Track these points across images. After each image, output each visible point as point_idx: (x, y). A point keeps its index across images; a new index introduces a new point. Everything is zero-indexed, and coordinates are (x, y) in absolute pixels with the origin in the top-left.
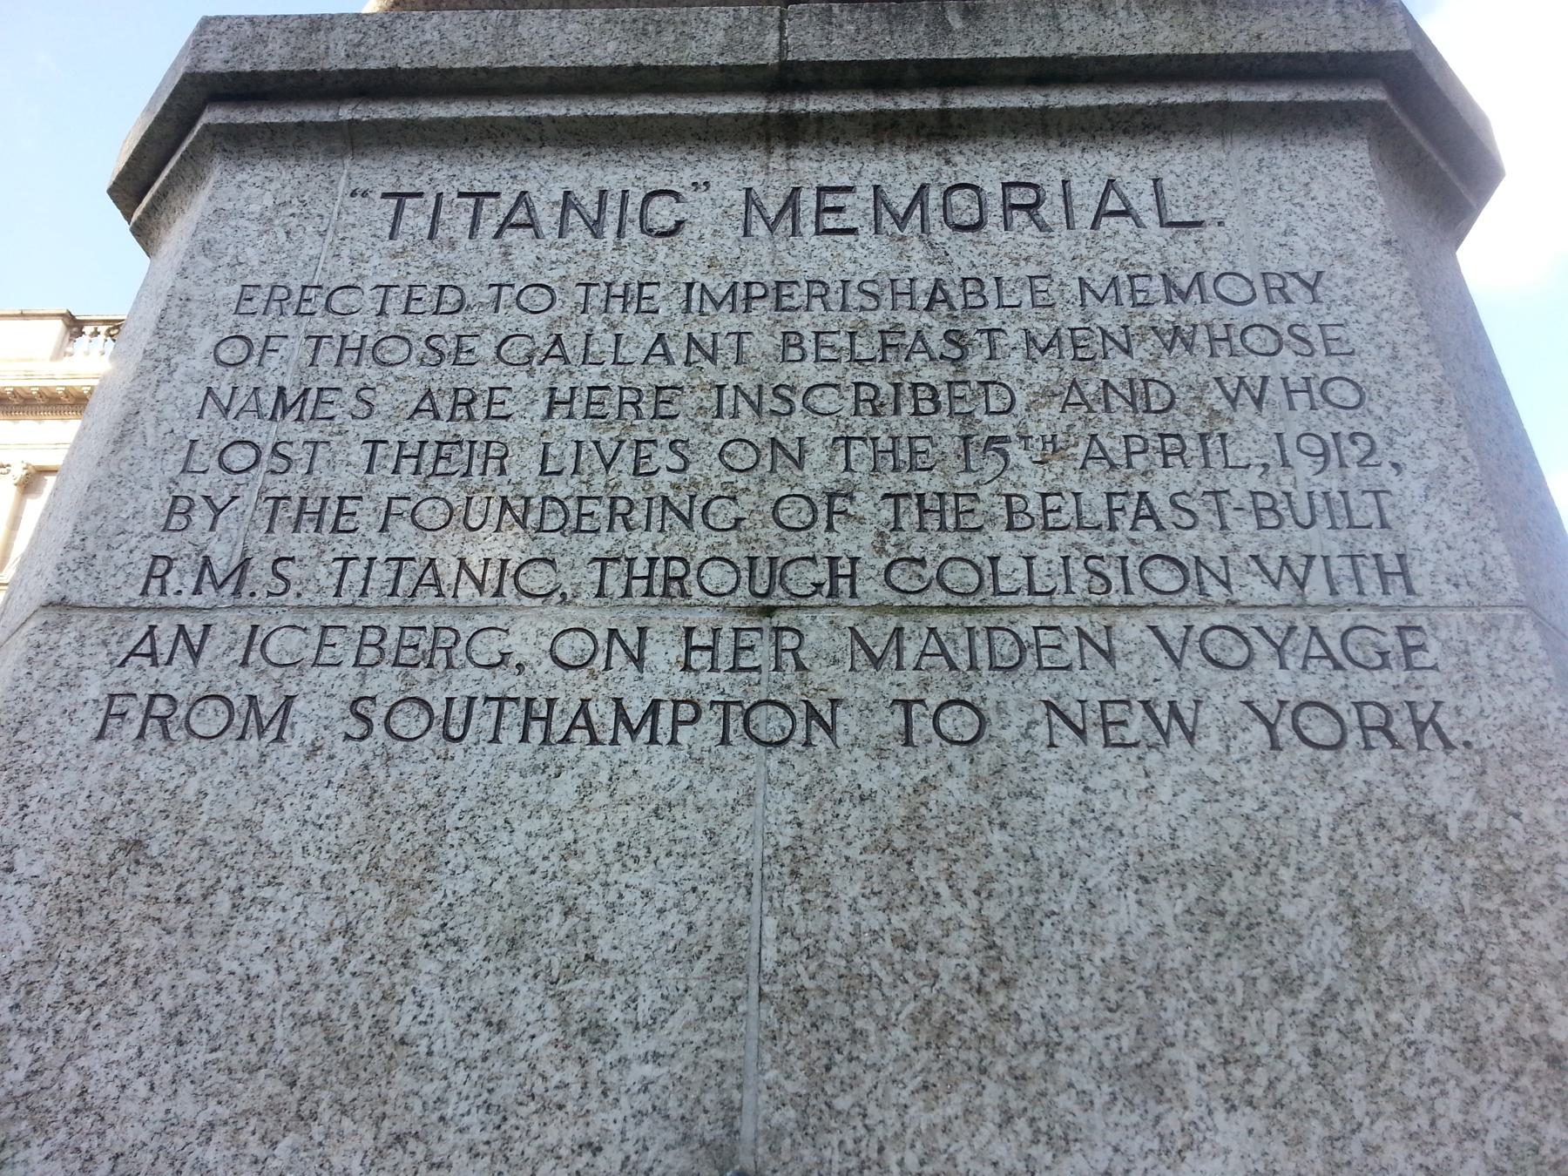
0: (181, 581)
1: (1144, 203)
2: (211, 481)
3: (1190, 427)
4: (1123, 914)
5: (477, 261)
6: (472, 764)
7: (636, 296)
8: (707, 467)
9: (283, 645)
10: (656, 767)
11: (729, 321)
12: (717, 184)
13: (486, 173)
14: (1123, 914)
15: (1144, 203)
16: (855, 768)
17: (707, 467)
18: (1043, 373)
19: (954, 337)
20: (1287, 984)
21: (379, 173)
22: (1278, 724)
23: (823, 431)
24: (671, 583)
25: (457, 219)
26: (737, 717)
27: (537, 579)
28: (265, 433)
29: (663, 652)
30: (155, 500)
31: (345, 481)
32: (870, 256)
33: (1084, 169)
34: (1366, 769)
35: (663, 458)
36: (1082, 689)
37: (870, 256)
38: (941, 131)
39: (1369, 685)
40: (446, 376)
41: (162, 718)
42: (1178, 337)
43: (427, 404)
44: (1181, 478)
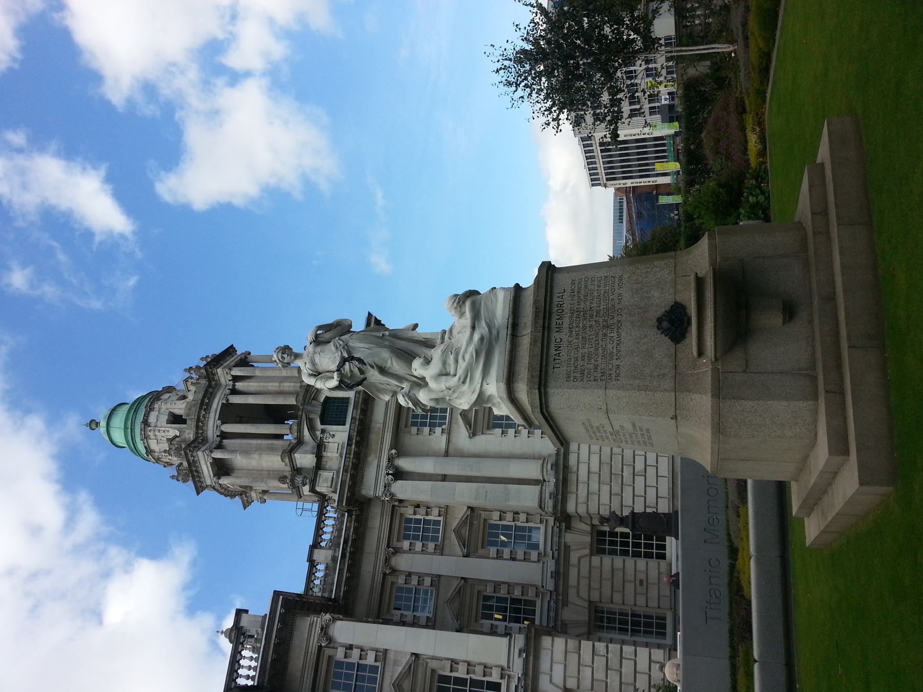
2: (592, 378)
12: (555, 335)
13: (551, 360)
21: (550, 370)
26: (619, 328)
31: (592, 366)
33: (556, 300)
34: (624, 281)
36: (617, 301)
37: (566, 321)
38: (550, 313)
44: (595, 293)
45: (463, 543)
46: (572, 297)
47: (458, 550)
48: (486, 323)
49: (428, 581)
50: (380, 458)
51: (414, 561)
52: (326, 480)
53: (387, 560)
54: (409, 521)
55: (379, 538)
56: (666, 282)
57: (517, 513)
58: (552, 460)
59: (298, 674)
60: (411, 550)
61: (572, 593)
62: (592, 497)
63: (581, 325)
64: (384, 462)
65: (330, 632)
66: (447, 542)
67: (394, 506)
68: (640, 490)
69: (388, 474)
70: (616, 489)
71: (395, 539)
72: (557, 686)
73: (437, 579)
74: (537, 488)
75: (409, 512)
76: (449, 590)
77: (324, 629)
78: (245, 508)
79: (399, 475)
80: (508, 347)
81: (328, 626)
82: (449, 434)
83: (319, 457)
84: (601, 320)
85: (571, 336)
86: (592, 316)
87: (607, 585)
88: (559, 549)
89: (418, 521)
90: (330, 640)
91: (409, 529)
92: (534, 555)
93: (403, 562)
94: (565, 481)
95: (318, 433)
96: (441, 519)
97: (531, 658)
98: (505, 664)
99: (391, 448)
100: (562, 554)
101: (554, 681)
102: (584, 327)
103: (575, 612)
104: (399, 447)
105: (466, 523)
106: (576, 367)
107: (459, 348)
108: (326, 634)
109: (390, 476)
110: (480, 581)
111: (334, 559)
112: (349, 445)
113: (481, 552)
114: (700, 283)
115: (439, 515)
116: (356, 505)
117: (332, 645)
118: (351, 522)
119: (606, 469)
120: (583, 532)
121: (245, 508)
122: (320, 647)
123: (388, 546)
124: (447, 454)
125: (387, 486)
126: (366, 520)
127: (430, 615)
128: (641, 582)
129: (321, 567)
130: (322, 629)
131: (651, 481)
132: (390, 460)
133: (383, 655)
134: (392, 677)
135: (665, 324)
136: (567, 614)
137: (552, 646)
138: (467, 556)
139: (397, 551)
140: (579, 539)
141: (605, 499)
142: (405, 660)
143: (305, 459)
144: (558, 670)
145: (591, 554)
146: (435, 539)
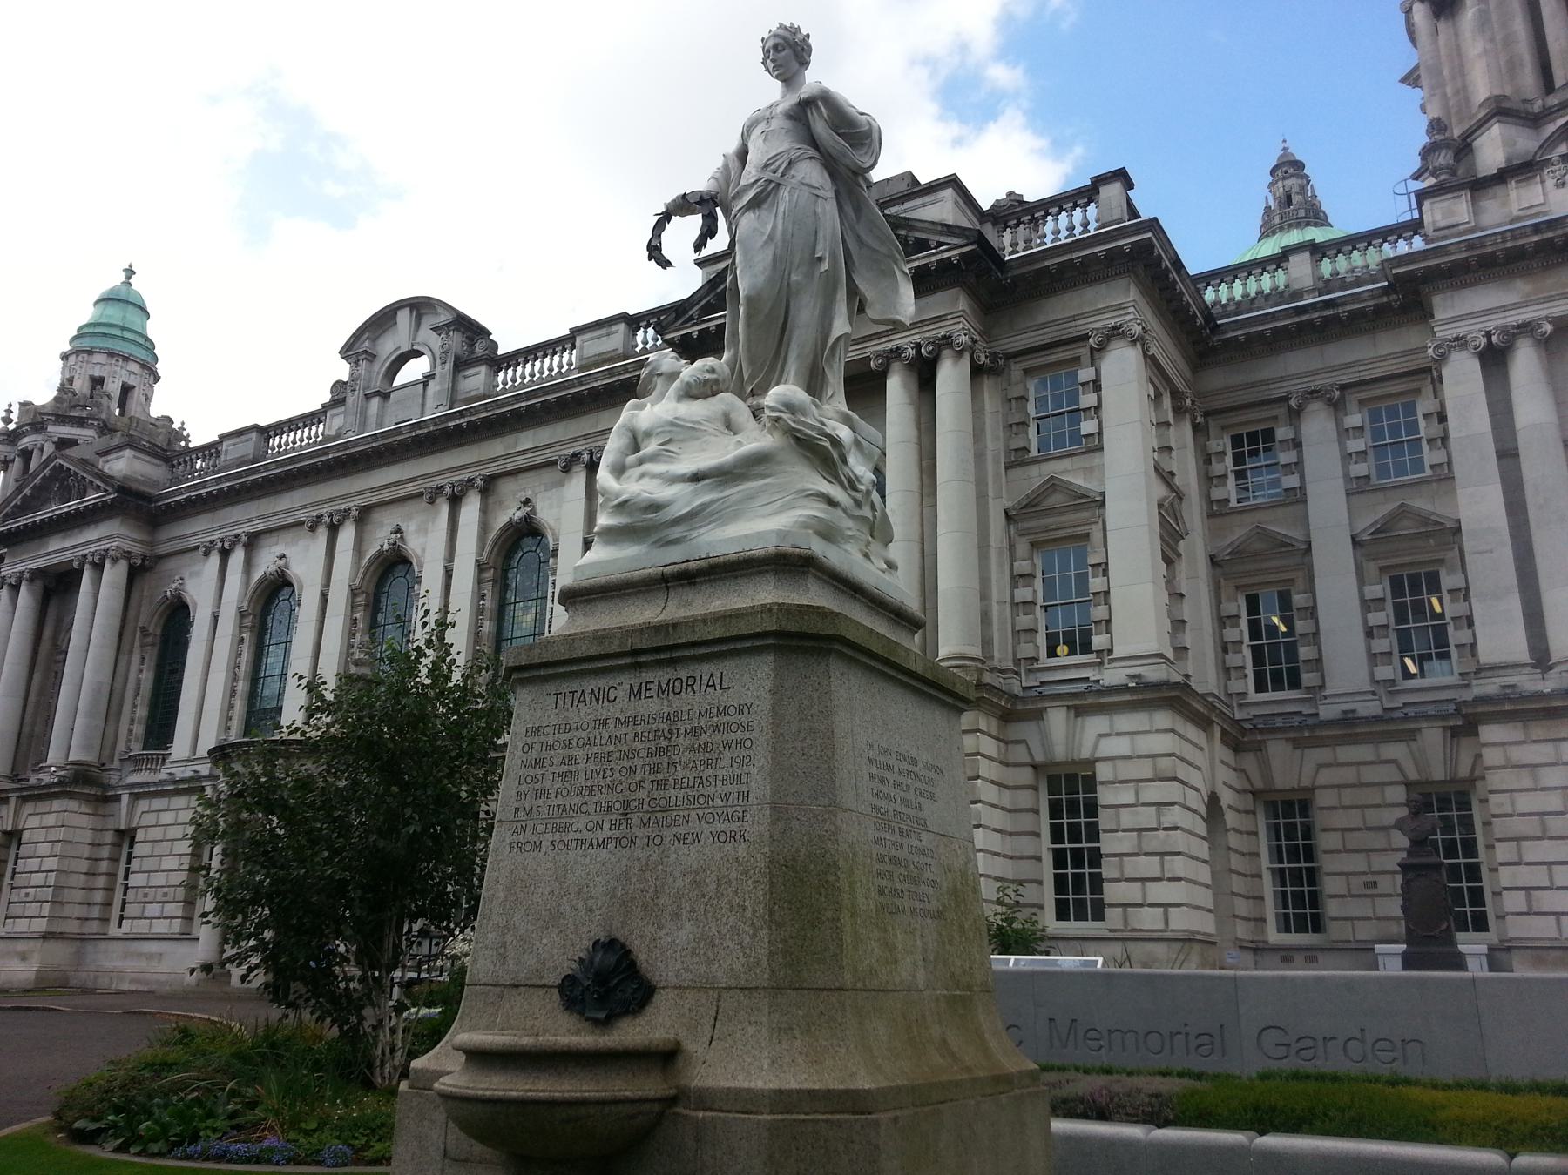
0: (521, 814)
1: (717, 681)
2: (522, 788)
3: (714, 756)
4: (680, 883)
6: (572, 855)
8: (617, 775)
9: (540, 828)
10: (604, 853)
11: (624, 730)
12: (625, 681)
15: (717, 681)
16: (639, 853)
17: (617, 775)
18: (687, 742)
19: (670, 732)
20: (704, 896)
21: (552, 688)
22: (715, 837)
23: (639, 763)
27: (584, 809)
28: (532, 772)
29: (606, 826)
30: (514, 793)
31: (548, 784)
33: (704, 670)
34: (728, 847)
35: (609, 773)
36: (681, 831)
38: (673, 662)
39: (734, 826)
40: (568, 752)
42: (716, 728)
45: (1382, 530)
46: (706, 713)
48: (704, 506)
49: (1291, 481)
50: (1526, 304)
51: (1323, 451)
52: (1452, 213)
53: (1313, 394)
54: (1410, 409)
55: (1356, 364)
56: (709, 963)
59: (1041, 319)
60: (1344, 433)
61: (1323, 754)
63: (638, 745)
64: (1515, 318)
65: (1114, 344)
66: (1380, 495)
67: (1428, 370)
69: (1488, 335)
71: (1363, 395)
72: (1096, 747)
73: (1297, 498)
75: (1425, 405)
76: (1281, 525)
77: (1116, 333)
78: (1403, 80)
79: (1494, 358)
81: (1122, 335)
83: (1502, 177)
84: (643, 794)
87: (1353, 819)
88: (1406, 718)
89: (1413, 427)
90: (1102, 348)
91: (1393, 413)
92: (1384, 672)
93: (1317, 426)
97: (1127, 697)
99: (1555, 321)
100: (1392, 725)
101: (1103, 741)
102: (633, 753)
103: (1287, 767)
105: (1426, 524)
106: (552, 746)
107: (670, 457)
109: (1484, 341)
110: (1311, 579)
111: (1297, 295)
112: (1536, 228)
113: (1371, 568)
114: (667, 1057)
115: (1432, 467)
116: (1408, 295)
118: (1373, 298)
120: (1452, 760)
121: (1403, 80)
122: (1086, 337)
123: (1344, 388)
125: (1460, 342)
127: (1233, 503)
128: (1374, 884)
129: (1281, 278)
130: (1115, 328)
132: (1526, 328)
133: (1094, 444)
134: (1066, 471)
136: (1278, 750)
137: (1158, 731)
138: (1356, 542)
139: (1337, 407)
140: (1431, 754)
141: (1525, 803)
143: (1492, 150)
144: (1119, 746)
145: (1409, 785)
146: (1383, 471)
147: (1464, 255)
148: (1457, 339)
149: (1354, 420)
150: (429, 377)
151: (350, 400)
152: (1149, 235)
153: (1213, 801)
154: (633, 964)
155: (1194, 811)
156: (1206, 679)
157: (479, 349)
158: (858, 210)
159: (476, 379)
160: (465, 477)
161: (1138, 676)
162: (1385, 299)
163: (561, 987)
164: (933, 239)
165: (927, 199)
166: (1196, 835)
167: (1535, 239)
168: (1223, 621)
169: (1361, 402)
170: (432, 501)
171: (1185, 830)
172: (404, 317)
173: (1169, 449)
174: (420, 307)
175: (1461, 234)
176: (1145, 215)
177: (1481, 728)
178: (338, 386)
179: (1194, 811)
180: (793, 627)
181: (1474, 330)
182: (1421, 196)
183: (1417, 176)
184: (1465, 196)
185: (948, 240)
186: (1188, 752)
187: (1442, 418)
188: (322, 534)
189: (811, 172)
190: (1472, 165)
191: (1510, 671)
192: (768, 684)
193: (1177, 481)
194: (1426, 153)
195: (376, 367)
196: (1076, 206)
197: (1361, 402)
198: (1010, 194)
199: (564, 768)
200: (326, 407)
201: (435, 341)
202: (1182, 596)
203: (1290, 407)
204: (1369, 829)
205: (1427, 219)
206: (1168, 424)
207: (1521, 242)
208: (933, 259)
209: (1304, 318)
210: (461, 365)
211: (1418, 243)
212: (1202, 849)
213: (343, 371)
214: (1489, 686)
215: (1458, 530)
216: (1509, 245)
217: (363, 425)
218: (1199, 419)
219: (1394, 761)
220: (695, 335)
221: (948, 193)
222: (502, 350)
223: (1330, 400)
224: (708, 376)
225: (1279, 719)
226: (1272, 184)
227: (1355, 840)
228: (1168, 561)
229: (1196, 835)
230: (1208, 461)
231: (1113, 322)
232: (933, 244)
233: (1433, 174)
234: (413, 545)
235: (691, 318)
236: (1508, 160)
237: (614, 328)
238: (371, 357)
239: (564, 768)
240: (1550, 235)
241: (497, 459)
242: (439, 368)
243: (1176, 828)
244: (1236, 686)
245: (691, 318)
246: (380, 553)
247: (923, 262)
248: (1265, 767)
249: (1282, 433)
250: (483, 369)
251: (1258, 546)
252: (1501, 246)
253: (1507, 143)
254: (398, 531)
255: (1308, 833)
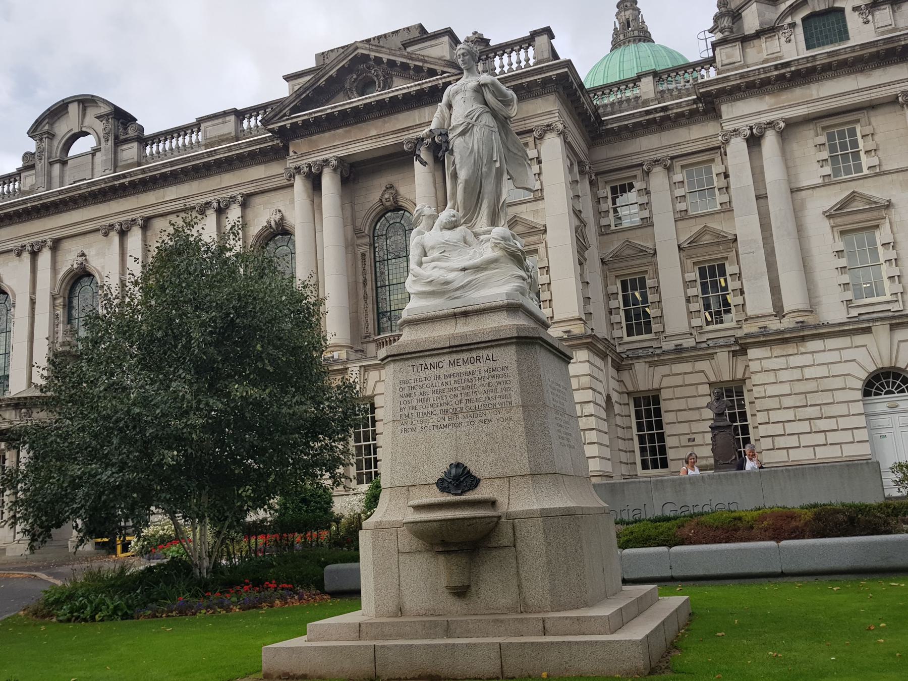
2: (403, 406)
5: (423, 374)
7: (439, 377)
12: (446, 359)
13: (421, 361)
14: (485, 438)
21: (410, 363)
23: (459, 393)
24: (446, 411)
25: (419, 369)
26: (454, 425)
29: (447, 419)
32: (463, 369)
33: (484, 353)
36: (482, 419)
37: (463, 369)
40: (422, 390)
41: (405, 430)
43: (421, 394)
46: (488, 371)
47: (684, 238)
48: (470, 282)
50: (771, 110)
53: (656, 162)
55: (679, 144)
57: (742, 292)
58: (810, 319)
60: (674, 185)
61: (665, 369)
62: (770, 377)
64: (765, 118)
67: (719, 148)
68: (790, 428)
69: (751, 128)
70: (787, 402)
74: (770, 310)
76: (638, 239)
77: (549, 128)
79: (754, 141)
80: (441, 313)
81: (552, 130)
82: (824, 185)
83: (758, 35)
84: (462, 405)
85: (446, 376)
86: (467, 394)
87: (681, 404)
88: (709, 347)
90: (541, 137)
92: (697, 322)
94: (785, 341)
95: (789, 20)
96: (719, 207)
98: (556, 318)
99: (785, 121)
100: (702, 352)
103: (644, 377)
104: (789, 129)
106: (414, 388)
107: (447, 259)
108: (545, 132)
109: (749, 132)
110: (656, 270)
111: (646, 103)
112: (776, 67)
113: (689, 263)
114: (493, 503)
115: (721, 204)
117: (538, 142)
119: (811, 386)
120: (733, 369)
122: (531, 131)
123: (672, 158)
124: (794, 191)
126: (695, 122)
127: (613, 228)
128: (693, 440)
130: (548, 126)
131: (806, 440)
132: (771, 124)
135: (453, 471)
136: (640, 367)
138: (680, 248)
139: (669, 169)
140: (722, 367)
141: (771, 390)
142: (539, 221)
145: (711, 384)
147: (738, 82)
148: (735, 131)
149: (678, 177)
150: (94, 152)
151: (39, 166)
152: (566, 70)
153: (609, 398)
154: (469, 471)
155: (600, 406)
156: (602, 331)
157: (131, 132)
158: (506, 135)
159: (130, 152)
160: (130, 218)
161: (569, 332)
162: (695, 106)
163: (437, 484)
164: (439, 69)
165: (433, 42)
166: (601, 419)
167: (776, 73)
168: (610, 296)
169: (682, 167)
170: (106, 235)
171: (596, 416)
172: (73, 109)
173: (578, 196)
174: (86, 102)
175: (736, 69)
176: (563, 57)
177: (748, 351)
178: (27, 156)
179: (600, 406)
180: (522, 334)
181: (743, 125)
182: (714, 45)
183: (711, 31)
184: (738, 45)
185: (449, 70)
186: (596, 373)
187: (726, 176)
188: (26, 257)
189: (487, 119)
190: (741, 28)
191: (763, 319)
192: (515, 358)
193: (583, 215)
194: (717, 19)
195: (55, 143)
196: (521, 48)
197: (682, 167)
198: (475, 33)
199: (421, 397)
200: (20, 172)
201: (99, 126)
202: (588, 283)
203: (643, 170)
204: (690, 409)
205: (718, 59)
206: (577, 182)
207: (768, 75)
208: (440, 82)
209: (651, 116)
210: (119, 142)
211: (712, 74)
212: (604, 426)
213: (31, 146)
214: (750, 328)
215: (736, 240)
216: (762, 76)
217: (49, 186)
218: (593, 177)
219: (703, 371)
220: (288, 126)
221: (446, 39)
222: (147, 133)
223: (665, 165)
224: (453, 219)
225: (640, 351)
226: (617, 14)
227: (682, 416)
228: (581, 264)
229: (601, 419)
230: (598, 203)
231: (547, 121)
232: (439, 72)
233: (721, 31)
234: (95, 264)
235: (285, 115)
236: (761, 24)
237: (228, 118)
238: (51, 136)
239: (421, 397)
240: (783, 71)
241: (152, 206)
242: (103, 144)
243: (592, 415)
244: (617, 333)
245: (285, 115)
246: (70, 271)
247: (434, 83)
248: (634, 378)
249: (638, 185)
250: (135, 145)
251: (628, 252)
252: (758, 77)
253: (760, 14)
254: (83, 255)
255: (658, 412)
